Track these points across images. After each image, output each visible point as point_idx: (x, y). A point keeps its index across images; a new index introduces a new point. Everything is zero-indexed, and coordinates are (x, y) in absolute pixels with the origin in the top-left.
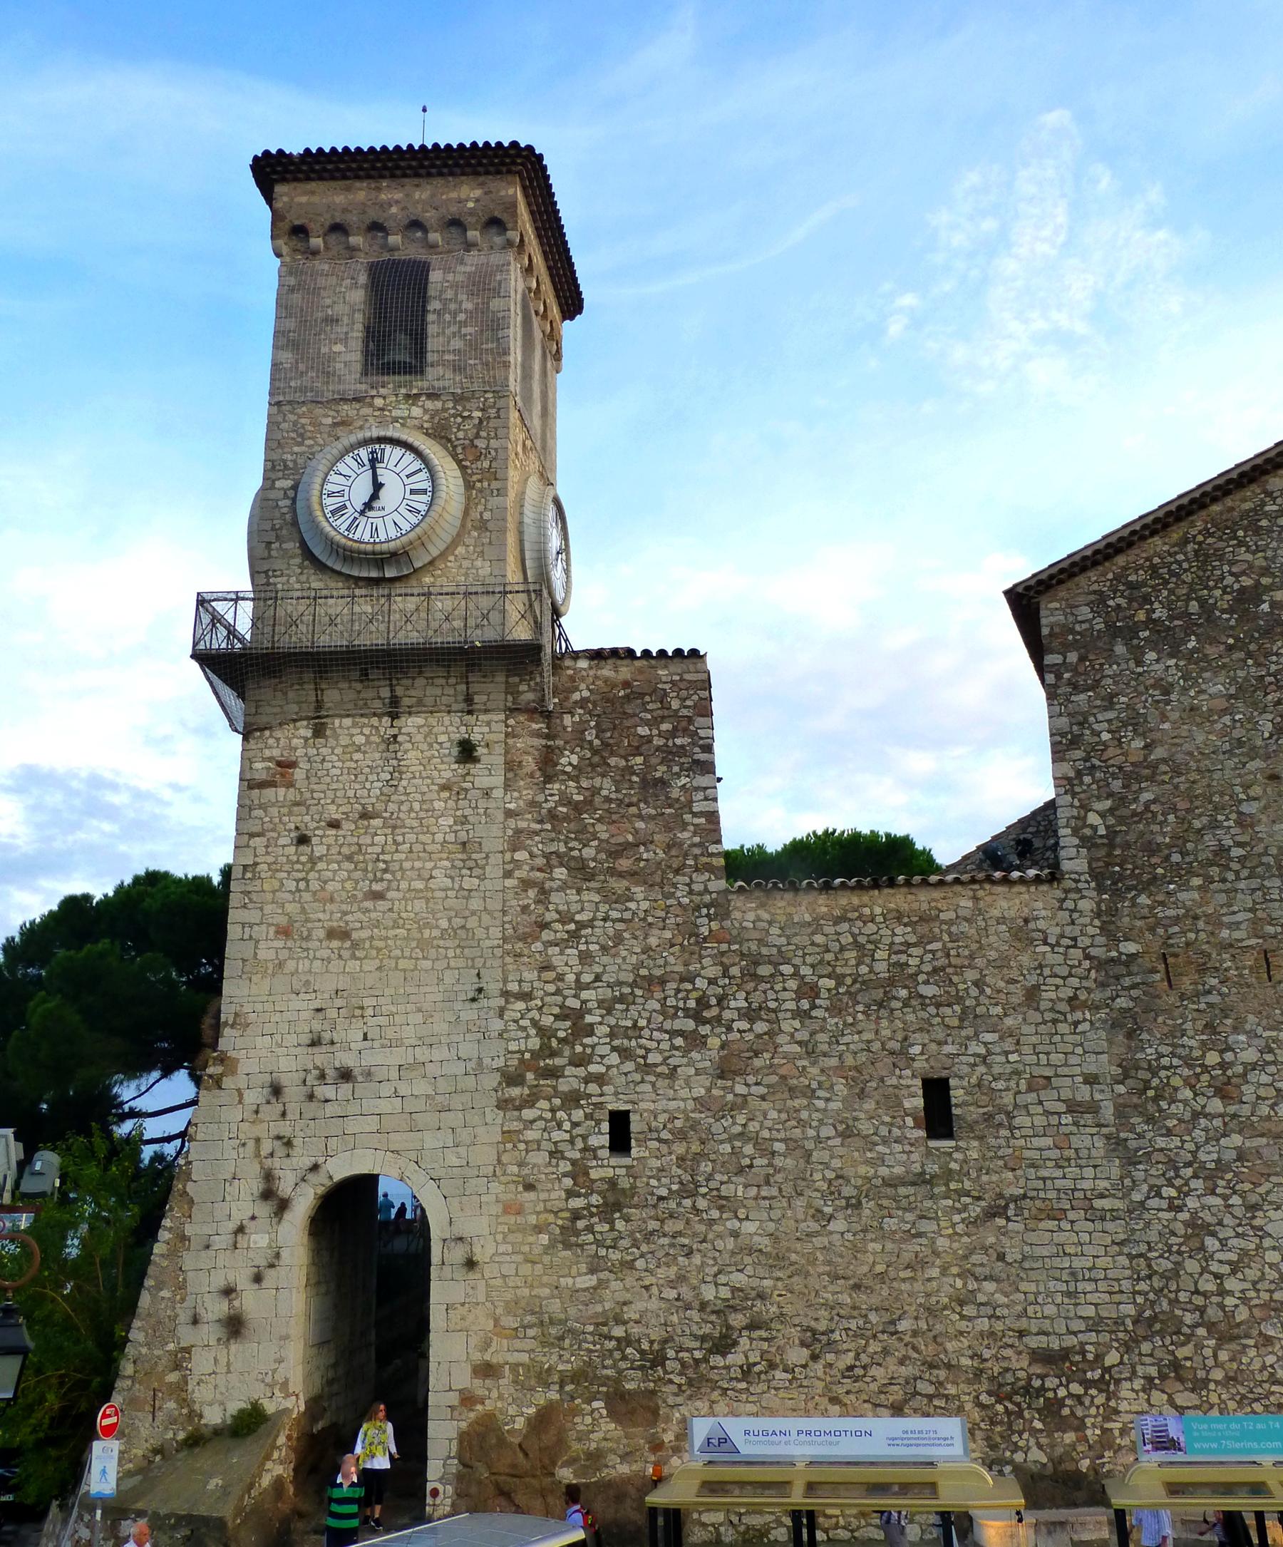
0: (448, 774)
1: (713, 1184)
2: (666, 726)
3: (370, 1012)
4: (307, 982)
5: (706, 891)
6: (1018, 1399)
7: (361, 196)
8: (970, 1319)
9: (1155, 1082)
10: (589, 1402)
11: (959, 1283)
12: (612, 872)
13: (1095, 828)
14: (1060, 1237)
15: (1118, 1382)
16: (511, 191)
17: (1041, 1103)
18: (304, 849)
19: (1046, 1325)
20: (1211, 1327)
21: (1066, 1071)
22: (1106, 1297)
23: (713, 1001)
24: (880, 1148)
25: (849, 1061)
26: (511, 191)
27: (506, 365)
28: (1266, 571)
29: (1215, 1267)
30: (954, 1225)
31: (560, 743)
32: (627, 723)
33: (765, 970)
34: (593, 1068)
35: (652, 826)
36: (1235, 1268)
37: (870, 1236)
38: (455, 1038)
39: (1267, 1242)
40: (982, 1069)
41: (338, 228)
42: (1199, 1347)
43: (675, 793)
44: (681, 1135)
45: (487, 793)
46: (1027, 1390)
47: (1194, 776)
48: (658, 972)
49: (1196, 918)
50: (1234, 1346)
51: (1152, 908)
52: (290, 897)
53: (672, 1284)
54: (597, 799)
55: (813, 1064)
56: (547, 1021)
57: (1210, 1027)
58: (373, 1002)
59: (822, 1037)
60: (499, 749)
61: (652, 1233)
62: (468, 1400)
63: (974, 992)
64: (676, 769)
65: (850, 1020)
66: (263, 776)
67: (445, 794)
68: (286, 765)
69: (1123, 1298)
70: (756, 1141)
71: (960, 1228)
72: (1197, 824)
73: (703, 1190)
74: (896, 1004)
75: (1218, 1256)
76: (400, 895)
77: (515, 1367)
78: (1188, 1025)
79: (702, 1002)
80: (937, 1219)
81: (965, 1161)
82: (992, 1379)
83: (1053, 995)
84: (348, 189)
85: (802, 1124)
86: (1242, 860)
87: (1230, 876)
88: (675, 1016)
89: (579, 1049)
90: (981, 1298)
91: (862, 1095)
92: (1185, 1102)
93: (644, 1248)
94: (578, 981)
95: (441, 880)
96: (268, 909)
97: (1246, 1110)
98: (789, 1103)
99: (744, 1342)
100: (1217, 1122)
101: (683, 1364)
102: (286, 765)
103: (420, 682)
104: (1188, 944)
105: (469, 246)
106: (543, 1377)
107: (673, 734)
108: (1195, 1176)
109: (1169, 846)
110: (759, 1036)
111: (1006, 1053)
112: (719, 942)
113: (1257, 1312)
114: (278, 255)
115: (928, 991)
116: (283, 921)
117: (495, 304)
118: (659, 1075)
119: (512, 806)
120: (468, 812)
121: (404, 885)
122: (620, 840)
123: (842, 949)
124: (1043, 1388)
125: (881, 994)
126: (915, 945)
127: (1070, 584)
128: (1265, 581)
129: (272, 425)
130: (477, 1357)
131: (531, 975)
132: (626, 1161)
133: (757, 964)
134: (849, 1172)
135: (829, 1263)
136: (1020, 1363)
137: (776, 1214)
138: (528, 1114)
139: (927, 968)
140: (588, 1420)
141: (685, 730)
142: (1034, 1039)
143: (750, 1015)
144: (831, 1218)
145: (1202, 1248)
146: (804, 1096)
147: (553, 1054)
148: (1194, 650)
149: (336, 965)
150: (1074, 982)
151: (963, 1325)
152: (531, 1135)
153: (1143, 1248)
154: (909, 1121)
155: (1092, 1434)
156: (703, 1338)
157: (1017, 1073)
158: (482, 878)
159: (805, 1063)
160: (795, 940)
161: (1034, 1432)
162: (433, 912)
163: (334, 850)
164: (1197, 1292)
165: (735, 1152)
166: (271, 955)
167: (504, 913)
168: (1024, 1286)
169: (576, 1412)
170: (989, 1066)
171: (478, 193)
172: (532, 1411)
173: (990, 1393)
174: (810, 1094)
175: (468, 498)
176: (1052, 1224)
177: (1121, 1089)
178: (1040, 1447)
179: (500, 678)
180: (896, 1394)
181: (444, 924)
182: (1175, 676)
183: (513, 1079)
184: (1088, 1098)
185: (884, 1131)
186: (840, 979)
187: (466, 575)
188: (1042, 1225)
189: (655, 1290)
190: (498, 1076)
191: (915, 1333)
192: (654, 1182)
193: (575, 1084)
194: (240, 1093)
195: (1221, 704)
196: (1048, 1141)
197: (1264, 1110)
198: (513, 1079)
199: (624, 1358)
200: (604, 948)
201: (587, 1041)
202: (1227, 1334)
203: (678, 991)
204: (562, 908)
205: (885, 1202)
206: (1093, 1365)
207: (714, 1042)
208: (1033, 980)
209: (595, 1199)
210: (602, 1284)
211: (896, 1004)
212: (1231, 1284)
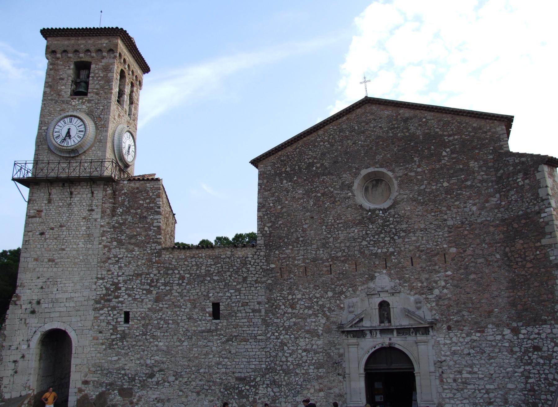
0: (85, 214)
1: (151, 332)
2: (148, 201)
3: (59, 283)
4: (42, 274)
5: (156, 249)
6: (231, 390)
7: (73, 42)
8: (220, 369)
9: (275, 304)
10: (113, 391)
11: (218, 359)
12: (130, 243)
13: (266, 231)
14: (246, 347)
15: (259, 385)
16: (116, 41)
17: (245, 310)
18: (44, 236)
19: (241, 370)
20: (284, 370)
21: (253, 301)
22: (258, 363)
23: (155, 281)
24: (199, 322)
25: (192, 297)
26: (116, 41)
27: (111, 93)
28: (315, 158)
29: (286, 354)
30: (217, 343)
31: (117, 205)
32: (137, 200)
34: (120, 299)
35: (141, 230)
36: (291, 354)
37: (194, 346)
38: (82, 290)
39: (299, 348)
40: (229, 300)
41: (65, 51)
42: (280, 376)
43: (149, 220)
44: (143, 318)
45: (96, 220)
46: (234, 388)
47: (292, 217)
48: (140, 272)
49: (290, 257)
50: (289, 376)
51: (279, 254)
52: (38, 250)
53: (138, 359)
54: (127, 222)
55: (182, 299)
56: (108, 286)
57: (290, 288)
58: (60, 280)
59: (185, 291)
60: (100, 207)
61: (134, 345)
62: (80, 390)
63: (229, 278)
64: (150, 213)
65: (193, 286)
66: (32, 214)
67: (84, 220)
68: (40, 211)
69: (263, 363)
70: (164, 320)
71: (219, 344)
72: (292, 231)
73: (149, 334)
74: (206, 282)
75: (287, 351)
76: (69, 249)
77: (94, 381)
78: (285, 288)
79: (152, 281)
80: (213, 342)
81: (222, 326)
82: (225, 385)
83: (251, 279)
84: (69, 40)
85: (178, 315)
86: (302, 241)
87: (299, 246)
88: (144, 285)
89: (116, 294)
90: (224, 363)
91: (195, 307)
92: (282, 309)
93: (131, 349)
94: (118, 274)
95: (81, 245)
96: (32, 253)
97: (297, 311)
98: (174, 310)
99: (157, 375)
100: (290, 315)
101: (140, 381)
102: (40, 211)
103: (79, 187)
104: (287, 265)
105: (103, 57)
106: (101, 385)
107: (149, 203)
108: (283, 330)
109: (285, 237)
110: (167, 291)
111: (236, 296)
112: (158, 264)
113: (295, 367)
114: (48, 59)
115: (216, 278)
116: (36, 256)
117: (110, 75)
118: (138, 301)
119: (102, 224)
120: (90, 225)
121: (71, 246)
122: (132, 234)
123: (193, 266)
124: (238, 387)
125: (201, 279)
126: (213, 265)
127: (266, 160)
128: (315, 161)
129: (42, 110)
130: (83, 379)
131: (104, 273)
132: (128, 325)
133: (168, 270)
134: (190, 329)
135: (182, 354)
136: (233, 381)
137: (169, 340)
138: (101, 312)
139: (216, 271)
140: (113, 396)
141: (153, 202)
142: (244, 292)
143: (165, 284)
144: (184, 341)
145: (283, 349)
146: (178, 307)
147: (109, 295)
148: (296, 180)
149: (50, 270)
150: (257, 275)
151: (218, 370)
152: (102, 318)
153: (269, 349)
154: (207, 315)
155: (251, 399)
156: (146, 374)
157: (239, 301)
158: (93, 245)
159: (179, 298)
160: (180, 263)
161: (234, 399)
162: (78, 254)
163: (51, 236)
164: (281, 361)
165: (158, 323)
166: (32, 266)
167: (98, 255)
168: (235, 360)
169: (110, 394)
170: (231, 300)
171: (107, 41)
172: (98, 393)
173: (224, 389)
174: (180, 307)
175: (96, 133)
176: (245, 343)
177: (267, 306)
178: (236, 403)
179: (102, 186)
180: (198, 389)
181: (81, 258)
182: (290, 188)
183: (97, 302)
184: (258, 308)
185: (200, 317)
187: (94, 156)
188: (242, 343)
189: (134, 361)
190: (93, 302)
191: (205, 373)
192: (135, 331)
193: (115, 303)
194: (21, 305)
195: (301, 196)
196: (246, 320)
197: (301, 312)
198: (97, 302)
199: (124, 379)
200: (125, 265)
201: (119, 291)
202: (287, 372)
203: (145, 278)
204: (115, 253)
205: (199, 337)
206: (252, 381)
207: (154, 292)
208: (245, 275)
209: (119, 336)
210: (119, 359)
211: (206, 282)
212: (290, 359)
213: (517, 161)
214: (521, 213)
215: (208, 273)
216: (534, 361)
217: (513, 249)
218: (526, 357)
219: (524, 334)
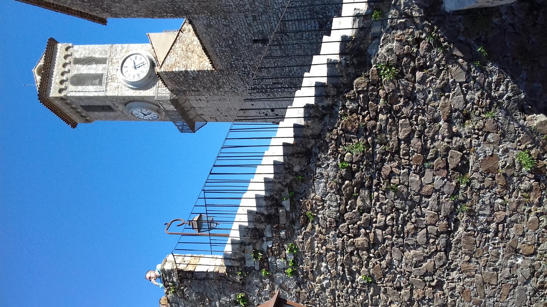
12: (218, 83)
33: (234, 66)
91: (261, 53)
107: (180, 76)
115: (231, 42)
143: (246, 68)
157: (248, 29)
186: (232, 56)
208: (221, 25)
215: (228, 46)
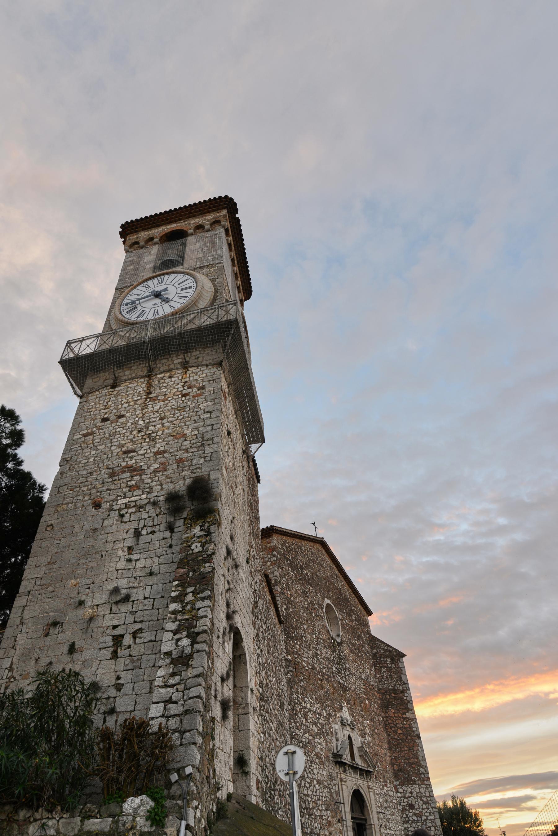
213: (386, 648)
214: (390, 687)
216: (411, 818)
217: (387, 715)
218: (405, 816)
219: (401, 793)
